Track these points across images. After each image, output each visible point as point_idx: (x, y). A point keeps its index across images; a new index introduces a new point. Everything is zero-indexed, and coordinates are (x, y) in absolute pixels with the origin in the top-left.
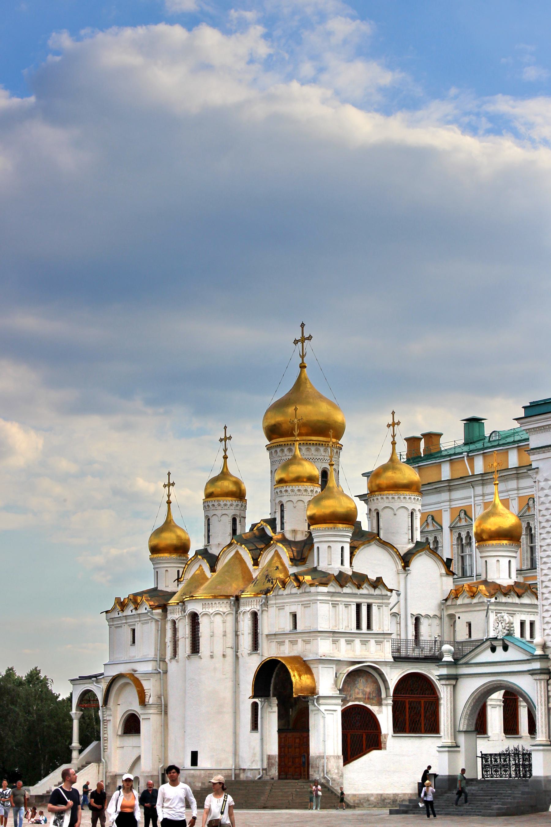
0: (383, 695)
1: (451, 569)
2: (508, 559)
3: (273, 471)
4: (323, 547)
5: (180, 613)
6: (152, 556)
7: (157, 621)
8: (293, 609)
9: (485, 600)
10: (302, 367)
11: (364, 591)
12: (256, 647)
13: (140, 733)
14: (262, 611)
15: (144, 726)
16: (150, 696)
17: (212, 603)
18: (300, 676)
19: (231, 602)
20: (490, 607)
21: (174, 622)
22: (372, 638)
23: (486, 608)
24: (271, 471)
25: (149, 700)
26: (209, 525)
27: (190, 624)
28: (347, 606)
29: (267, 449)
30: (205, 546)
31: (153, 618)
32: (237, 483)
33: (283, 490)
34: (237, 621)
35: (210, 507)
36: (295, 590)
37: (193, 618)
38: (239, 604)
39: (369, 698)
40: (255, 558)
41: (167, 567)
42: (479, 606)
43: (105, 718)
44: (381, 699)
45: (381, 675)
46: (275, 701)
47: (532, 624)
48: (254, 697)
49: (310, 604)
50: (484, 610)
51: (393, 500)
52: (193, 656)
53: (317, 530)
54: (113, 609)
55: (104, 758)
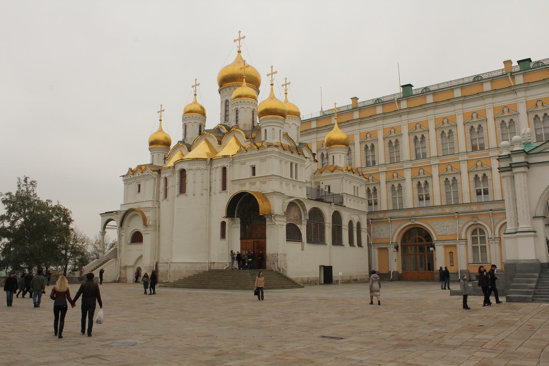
0: (303, 219)
1: (316, 158)
2: (344, 155)
3: (224, 101)
4: (269, 129)
5: (170, 173)
6: (150, 147)
7: (155, 179)
8: (253, 163)
9: (341, 172)
10: (239, 52)
11: (293, 155)
12: (224, 188)
13: (142, 242)
14: (230, 166)
15: (146, 238)
16: (150, 221)
18: (263, 202)
19: (207, 163)
20: (344, 177)
21: (166, 179)
22: (298, 184)
23: (343, 177)
24: (222, 102)
25: (149, 223)
26: (186, 129)
27: (179, 176)
28: (286, 163)
29: (219, 92)
30: (183, 139)
31: (153, 177)
32: (202, 108)
33: (238, 101)
34: (211, 174)
36: (253, 152)
37: (181, 173)
38: (211, 164)
39: (296, 220)
40: (218, 140)
42: (337, 176)
43: (120, 234)
44: (302, 221)
45: (303, 206)
46: (238, 221)
50: (339, 178)
51: (289, 120)
52: (180, 195)
53: (266, 119)
54: (127, 175)
55: (119, 257)
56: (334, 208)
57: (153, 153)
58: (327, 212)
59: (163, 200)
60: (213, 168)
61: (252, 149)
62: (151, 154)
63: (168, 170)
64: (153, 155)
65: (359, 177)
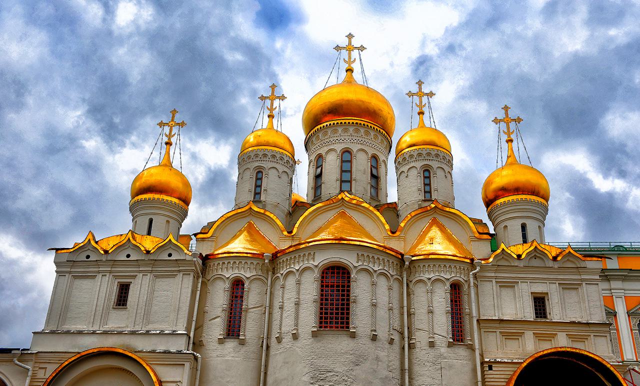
8: (539, 288)
17: (373, 257)
21: (238, 285)
33: (433, 153)
35: (269, 156)
41: (169, 216)
49: (580, 284)
59: (221, 341)
60: (420, 281)
61: (533, 255)
63: (249, 262)
64: (151, 221)
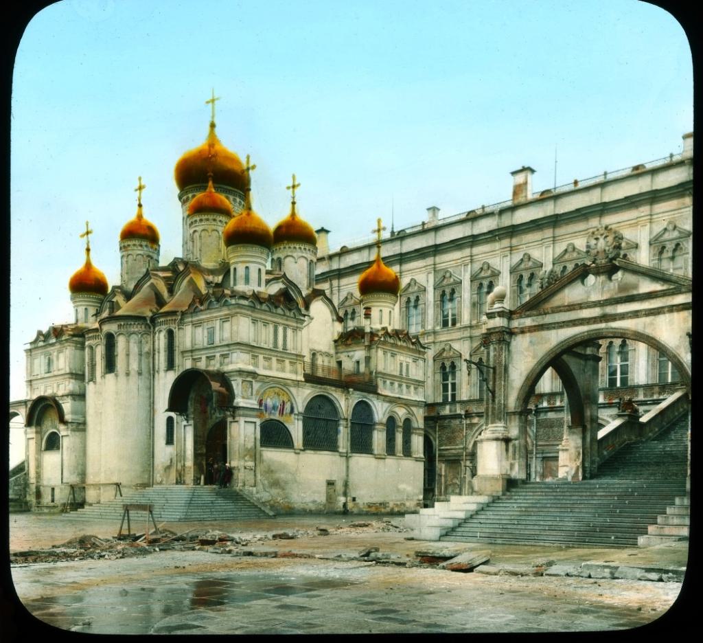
47: (407, 366)
48: (170, 409)
54: (35, 341)
56: (356, 397)
57: (77, 306)
58: (345, 403)
62: (74, 307)
64: (77, 310)
65: (411, 346)
